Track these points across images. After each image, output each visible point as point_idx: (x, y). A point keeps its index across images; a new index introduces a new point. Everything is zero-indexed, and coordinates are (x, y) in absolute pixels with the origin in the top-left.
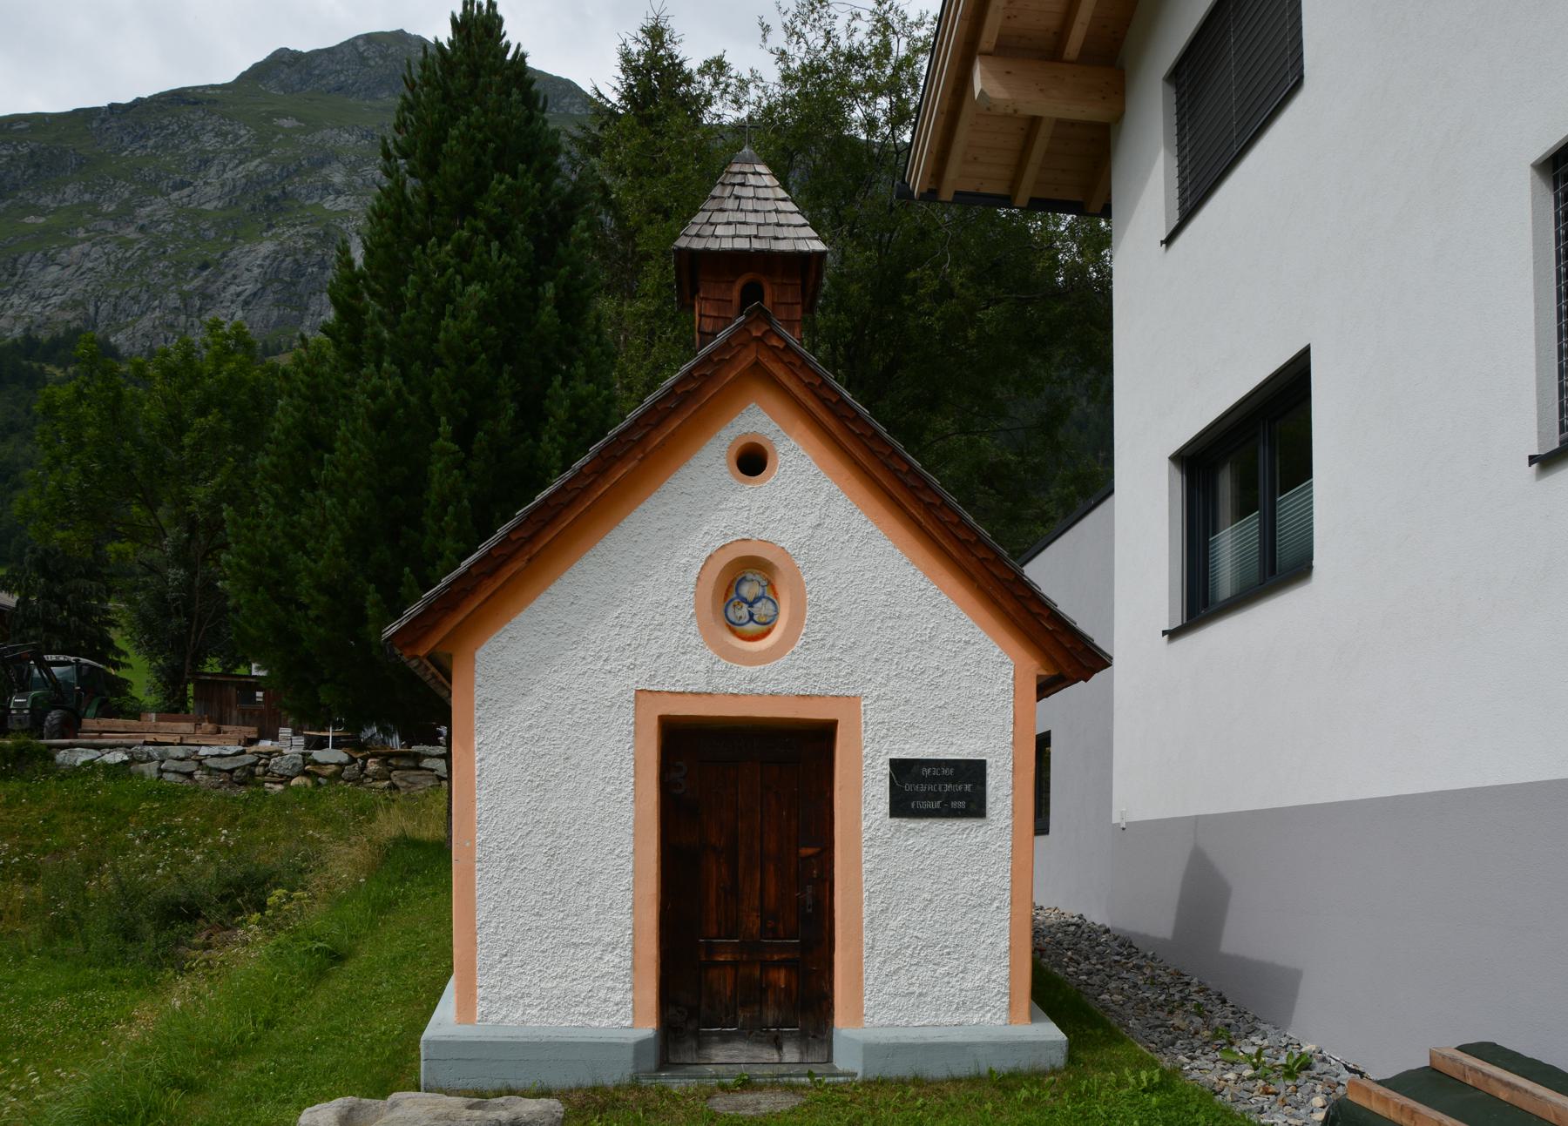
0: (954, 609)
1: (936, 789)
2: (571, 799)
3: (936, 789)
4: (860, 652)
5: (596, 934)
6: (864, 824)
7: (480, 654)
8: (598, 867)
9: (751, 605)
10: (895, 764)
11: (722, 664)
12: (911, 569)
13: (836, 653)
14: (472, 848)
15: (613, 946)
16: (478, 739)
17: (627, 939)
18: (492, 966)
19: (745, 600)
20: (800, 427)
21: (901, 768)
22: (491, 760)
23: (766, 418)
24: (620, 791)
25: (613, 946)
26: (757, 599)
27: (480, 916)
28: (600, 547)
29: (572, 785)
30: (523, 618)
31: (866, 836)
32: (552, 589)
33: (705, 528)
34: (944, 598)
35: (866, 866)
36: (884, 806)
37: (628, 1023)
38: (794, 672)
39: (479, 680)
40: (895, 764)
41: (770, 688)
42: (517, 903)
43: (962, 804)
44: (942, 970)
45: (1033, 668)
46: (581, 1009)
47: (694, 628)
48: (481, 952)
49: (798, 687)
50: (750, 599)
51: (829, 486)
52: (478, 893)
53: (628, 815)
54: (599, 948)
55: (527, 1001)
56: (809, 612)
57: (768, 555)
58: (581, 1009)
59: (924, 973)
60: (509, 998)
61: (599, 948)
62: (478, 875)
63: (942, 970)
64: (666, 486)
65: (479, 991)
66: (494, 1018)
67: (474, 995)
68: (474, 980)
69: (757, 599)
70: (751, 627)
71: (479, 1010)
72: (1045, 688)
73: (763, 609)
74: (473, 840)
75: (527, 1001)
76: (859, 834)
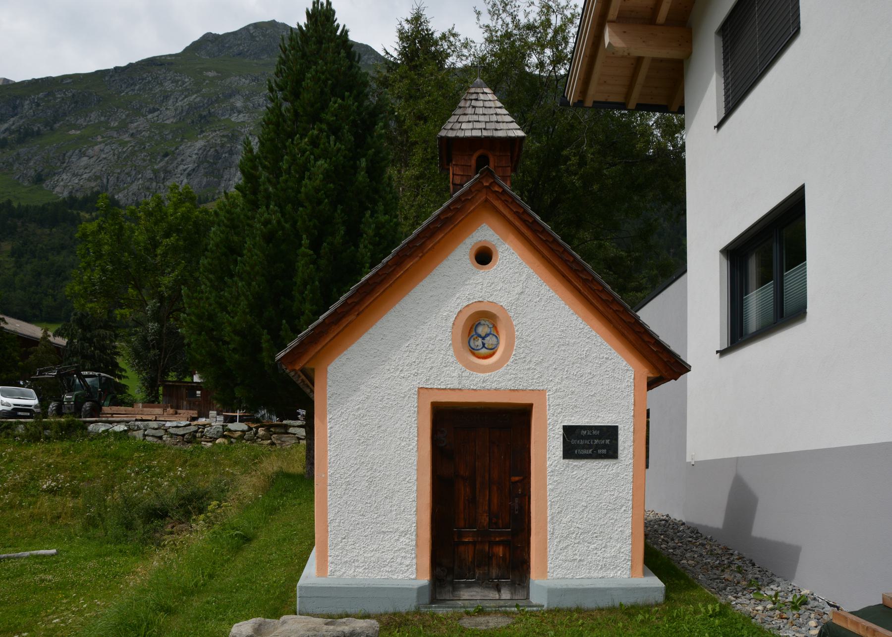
0: (600, 339)
1: (590, 443)
2: (382, 450)
3: (590, 443)
4: (545, 365)
5: (396, 526)
6: (548, 463)
7: (330, 368)
8: (397, 488)
9: (483, 338)
10: (566, 428)
12: (575, 317)
13: (532, 366)
14: (326, 478)
15: (405, 533)
16: (329, 416)
17: (413, 529)
18: (337, 544)
19: (480, 336)
20: (512, 237)
21: (570, 432)
22: (336, 428)
23: (491, 232)
25: (405, 533)
26: (487, 335)
27: (330, 516)
29: (382, 442)
31: (549, 470)
32: (371, 331)
33: (457, 295)
34: (594, 333)
36: (560, 452)
37: (414, 577)
38: (508, 377)
39: (330, 383)
40: (566, 428)
41: (494, 386)
43: (604, 451)
44: (593, 546)
45: (645, 373)
46: (387, 568)
47: (451, 352)
49: (510, 385)
50: (483, 335)
51: (527, 270)
53: (414, 459)
55: (356, 564)
58: (387, 568)
60: (346, 562)
62: (329, 493)
63: (593, 546)
64: (435, 272)
65: (329, 558)
66: (338, 573)
67: (326, 561)
68: (327, 552)
69: (487, 335)
70: (484, 351)
71: (329, 569)
72: (652, 384)
74: (326, 473)
75: (356, 564)
76: (546, 469)
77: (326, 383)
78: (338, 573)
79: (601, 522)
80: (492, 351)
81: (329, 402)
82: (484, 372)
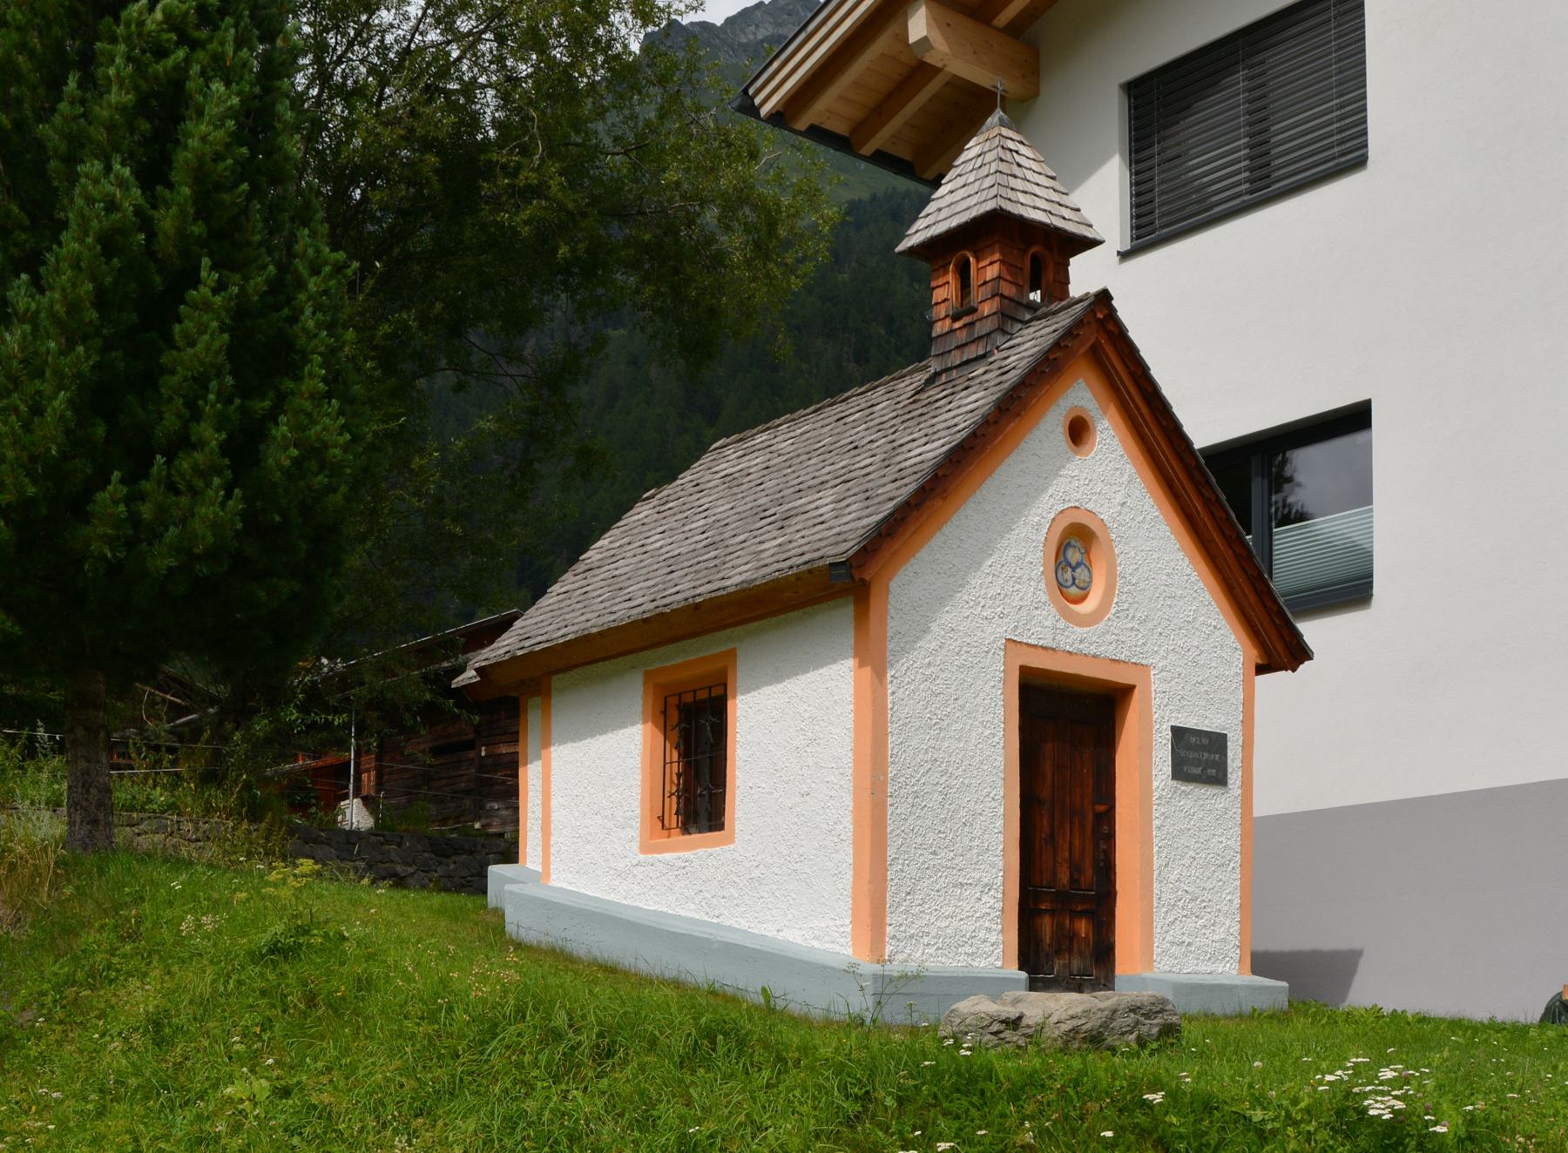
0: (1208, 596)
1: (1200, 757)
2: (959, 740)
3: (1200, 757)
4: (1150, 625)
5: (977, 875)
6: (1155, 784)
7: (893, 585)
8: (979, 808)
9: (1074, 569)
11: (1062, 624)
12: (1181, 555)
13: (1134, 624)
14: (885, 782)
15: (989, 886)
18: (900, 904)
19: (1069, 564)
20: (1113, 410)
21: (1179, 734)
22: (900, 694)
23: (1089, 395)
24: (994, 735)
25: (989, 887)
26: (1079, 564)
27: (891, 852)
28: (979, 495)
29: (958, 726)
30: (924, 555)
31: (1156, 795)
33: (1050, 491)
34: (1201, 584)
35: (1156, 823)
37: (999, 964)
38: (1109, 638)
39: (892, 611)
41: (1093, 650)
42: (919, 840)
44: (1201, 922)
45: (1254, 656)
46: (967, 949)
47: (1042, 586)
48: (891, 889)
49: (1110, 651)
50: (1073, 563)
51: (1130, 468)
52: (889, 829)
54: (979, 888)
55: (926, 940)
56: (1119, 582)
57: (1063, 523)
58: (967, 949)
59: (1190, 923)
60: (912, 937)
61: (979, 888)
63: (1201, 922)
64: (1023, 445)
65: (888, 929)
66: (900, 957)
67: (883, 934)
68: (884, 917)
69: (1079, 564)
70: (1073, 590)
73: (1081, 573)
74: (885, 774)
75: (926, 940)
76: (1151, 792)
77: (886, 611)
78: (900, 957)
79: (1209, 885)
80: (1085, 590)
81: (890, 646)
82: (1080, 625)
